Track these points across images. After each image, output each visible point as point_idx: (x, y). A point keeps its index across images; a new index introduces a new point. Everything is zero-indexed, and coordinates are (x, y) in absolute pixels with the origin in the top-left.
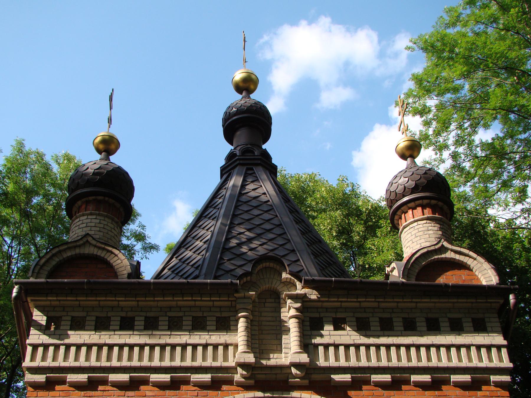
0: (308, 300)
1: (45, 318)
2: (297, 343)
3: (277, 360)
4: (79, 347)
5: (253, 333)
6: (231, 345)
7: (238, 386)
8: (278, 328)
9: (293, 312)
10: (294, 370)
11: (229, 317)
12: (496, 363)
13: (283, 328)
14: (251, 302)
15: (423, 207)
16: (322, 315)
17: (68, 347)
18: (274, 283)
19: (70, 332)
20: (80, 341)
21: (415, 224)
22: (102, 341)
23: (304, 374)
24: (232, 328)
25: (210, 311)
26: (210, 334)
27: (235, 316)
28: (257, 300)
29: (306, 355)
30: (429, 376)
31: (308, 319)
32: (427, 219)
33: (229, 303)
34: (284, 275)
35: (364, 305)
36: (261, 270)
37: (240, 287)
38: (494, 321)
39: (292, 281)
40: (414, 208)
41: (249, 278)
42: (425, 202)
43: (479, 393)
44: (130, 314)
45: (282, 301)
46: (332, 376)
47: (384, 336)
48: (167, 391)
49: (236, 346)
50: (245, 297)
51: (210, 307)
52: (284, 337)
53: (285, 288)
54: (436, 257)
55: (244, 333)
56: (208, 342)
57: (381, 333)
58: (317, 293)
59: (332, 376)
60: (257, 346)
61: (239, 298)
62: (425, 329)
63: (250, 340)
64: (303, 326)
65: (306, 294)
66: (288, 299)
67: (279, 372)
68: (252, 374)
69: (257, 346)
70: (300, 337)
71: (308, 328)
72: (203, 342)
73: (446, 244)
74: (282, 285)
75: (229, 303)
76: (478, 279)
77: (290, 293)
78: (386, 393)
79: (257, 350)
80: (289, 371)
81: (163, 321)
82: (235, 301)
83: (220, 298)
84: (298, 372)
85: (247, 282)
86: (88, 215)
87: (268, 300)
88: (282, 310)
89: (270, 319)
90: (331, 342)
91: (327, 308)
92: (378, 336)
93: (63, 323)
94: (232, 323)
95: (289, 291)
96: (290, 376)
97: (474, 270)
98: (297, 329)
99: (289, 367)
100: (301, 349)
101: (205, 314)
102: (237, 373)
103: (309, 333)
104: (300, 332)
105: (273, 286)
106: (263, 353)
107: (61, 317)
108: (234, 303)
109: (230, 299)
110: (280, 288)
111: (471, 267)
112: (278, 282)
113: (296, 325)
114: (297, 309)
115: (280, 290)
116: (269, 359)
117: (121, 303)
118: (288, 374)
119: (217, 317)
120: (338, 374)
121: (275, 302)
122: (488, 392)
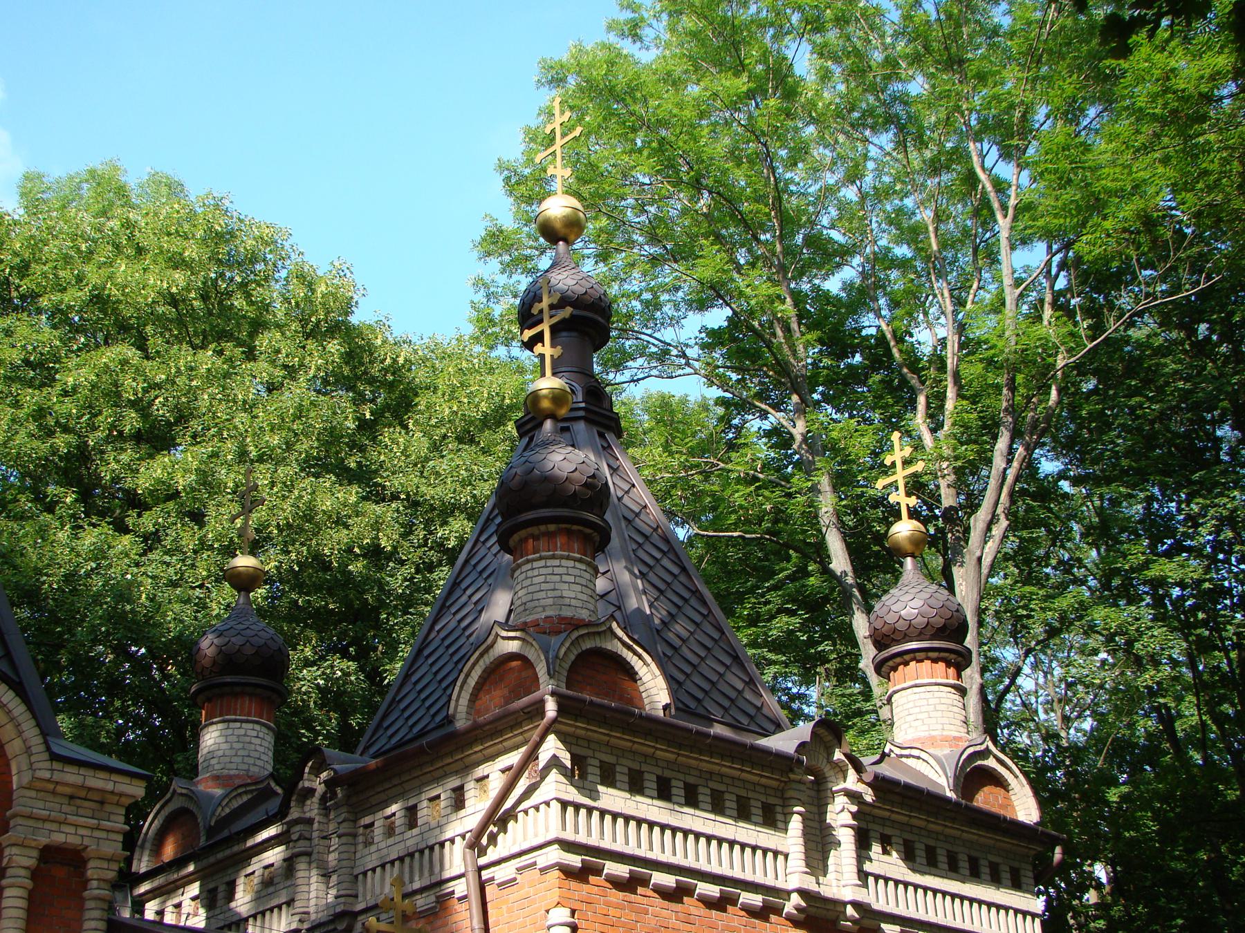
1: (568, 756)
4: (615, 816)
6: (781, 853)
9: (847, 818)
10: (850, 911)
17: (603, 813)
19: (601, 788)
24: (780, 825)
33: (774, 784)
44: (667, 774)
47: (930, 874)
48: (714, 912)
49: (786, 856)
50: (800, 782)
54: (979, 762)
57: (927, 869)
59: (883, 926)
61: (794, 781)
62: (967, 872)
81: (704, 796)
92: (923, 873)
93: (590, 769)
96: (842, 917)
99: (845, 904)
107: (585, 758)
110: (829, 772)
113: (852, 839)
117: (658, 752)
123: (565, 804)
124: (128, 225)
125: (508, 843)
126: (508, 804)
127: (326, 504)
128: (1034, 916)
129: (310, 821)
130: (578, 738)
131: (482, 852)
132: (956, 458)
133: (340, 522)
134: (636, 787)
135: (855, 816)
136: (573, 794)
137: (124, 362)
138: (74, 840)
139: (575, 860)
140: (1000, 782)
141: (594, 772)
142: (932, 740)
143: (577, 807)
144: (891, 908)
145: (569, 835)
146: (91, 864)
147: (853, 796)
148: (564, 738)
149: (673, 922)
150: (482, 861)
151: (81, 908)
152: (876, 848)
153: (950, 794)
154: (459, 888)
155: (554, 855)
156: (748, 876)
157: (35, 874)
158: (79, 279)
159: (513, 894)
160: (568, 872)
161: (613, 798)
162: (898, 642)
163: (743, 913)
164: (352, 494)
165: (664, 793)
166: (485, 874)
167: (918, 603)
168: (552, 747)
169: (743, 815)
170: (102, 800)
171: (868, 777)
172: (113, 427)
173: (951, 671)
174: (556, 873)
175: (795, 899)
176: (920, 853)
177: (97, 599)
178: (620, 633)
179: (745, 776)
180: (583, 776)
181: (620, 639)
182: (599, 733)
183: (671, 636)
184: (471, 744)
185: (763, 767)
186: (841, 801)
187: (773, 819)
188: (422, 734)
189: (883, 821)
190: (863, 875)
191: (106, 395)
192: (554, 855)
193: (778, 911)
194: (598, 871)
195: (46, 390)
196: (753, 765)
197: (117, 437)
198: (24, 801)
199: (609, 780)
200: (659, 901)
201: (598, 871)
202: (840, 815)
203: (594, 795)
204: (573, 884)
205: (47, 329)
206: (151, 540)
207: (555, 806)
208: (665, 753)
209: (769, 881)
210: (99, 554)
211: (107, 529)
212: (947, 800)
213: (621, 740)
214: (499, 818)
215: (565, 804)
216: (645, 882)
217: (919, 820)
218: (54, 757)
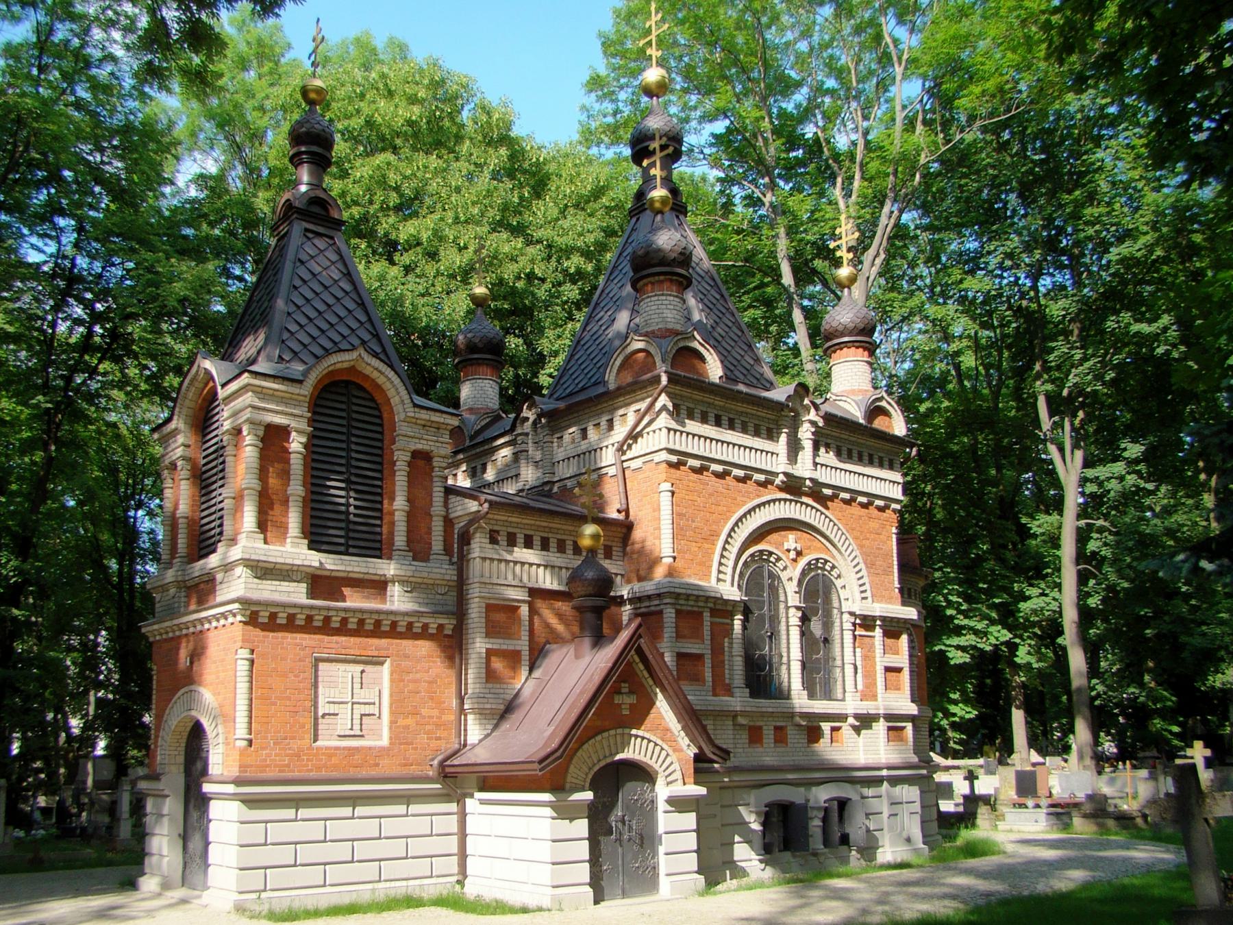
4: (694, 435)
10: (808, 483)
17: (688, 434)
44: (720, 413)
81: (738, 425)
110: (801, 411)
123: (669, 430)
124: (383, 76)
125: (638, 449)
126: (638, 429)
127: (506, 249)
129: (527, 434)
131: (624, 453)
132: (859, 218)
133: (514, 259)
134: (704, 420)
135: (813, 433)
136: (673, 425)
137: (389, 164)
138: (426, 448)
139: (674, 459)
141: (684, 412)
142: (853, 392)
143: (675, 431)
144: (828, 481)
145: (671, 446)
146: (436, 459)
147: (813, 423)
148: (670, 395)
149: (721, 489)
150: (624, 458)
151: (432, 481)
152: (822, 450)
153: (862, 421)
154: (612, 471)
155: (664, 456)
156: (759, 466)
157: (410, 464)
158: (358, 111)
159: (641, 476)
160: (671, 465)
161: (693, 426)
162: (838, 337)
164: (519, 243)
165: (718, 423)
166: (625, 464)
167: (851, 315)
168: (663, 400)
169: (757, 434)
170: (438, 427)
171: (822, 413)
172: (383, 202)
173: (866, 353)
174: (664, 465)
175: (781, 477)
176: (845, 453)
177: (383, 304)
180: (678, 415)
182: (686, 392)
183: (716, 335)
184: (618, 397)
185: (768, 409)
186: (806, 426)
187: (772, 436)
188: (583, 389)
189: (827, 436)
190: (815, 464)
191: (378, 183)
192: (664, 456)
193: (772, 483)
194: (685, 464)
195: (346, 181)
196: (764, 407)
197: (385, 209)
198: (402, 428)
199: (691, 417)
200: (714, 478)
201: (685, 464)
202: (806, 433)
203: (683, 425)
204: (673, 471)
205: (342, 143)
206: (408, 269)
207: (665, 431)
208: (719, 402)
209: (769, 468)
210: (382, 278)
211: (386, 263)
212: (861, 425)
213: (698, 395)
214: (634, 436)
215: (669, 430)
216: (707, 469)
217: (845, 435)
218: (415, 405)
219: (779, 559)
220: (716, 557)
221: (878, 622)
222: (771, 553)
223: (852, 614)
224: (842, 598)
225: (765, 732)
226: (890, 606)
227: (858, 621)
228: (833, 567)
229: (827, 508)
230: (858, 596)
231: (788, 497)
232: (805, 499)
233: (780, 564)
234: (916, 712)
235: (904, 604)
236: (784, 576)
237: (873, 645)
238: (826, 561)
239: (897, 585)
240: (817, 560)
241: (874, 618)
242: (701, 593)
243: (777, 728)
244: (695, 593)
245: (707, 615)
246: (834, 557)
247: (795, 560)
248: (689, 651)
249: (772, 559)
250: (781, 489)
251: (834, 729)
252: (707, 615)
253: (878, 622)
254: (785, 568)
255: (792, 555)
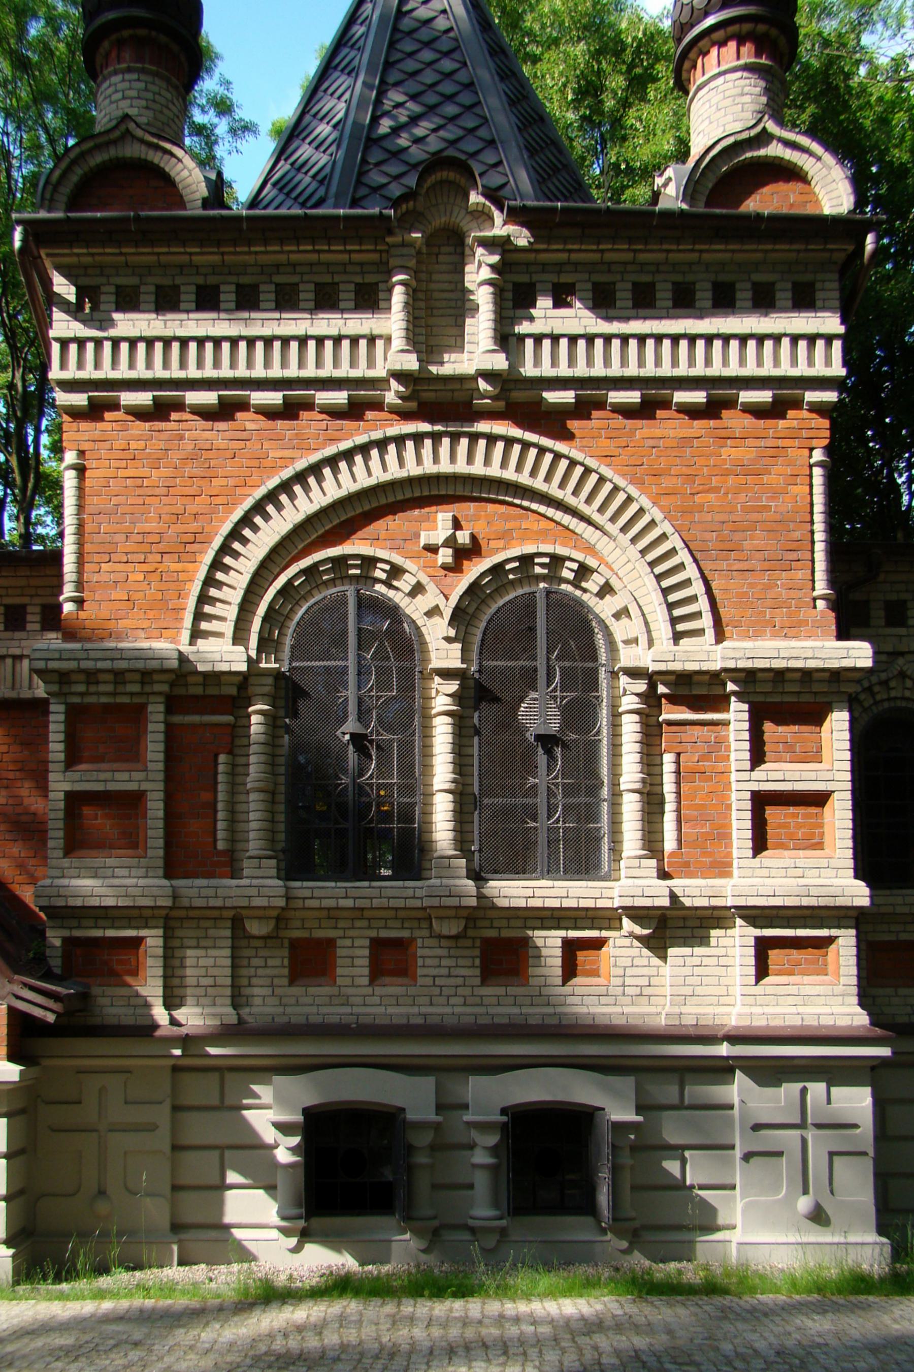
0: (512, 247)
2: (490, 333)
3: (455, 365)
4: (133, 342)
5: (418, 313)
6: (380, 337)
7: (391, 412)
8: (459, 303)
10: (483, 385)
11: (377, 284)
12: (820, 370)
13: (468, 305)
14: (413, 252)
15: (741, 41)
16: (535, 278)
17: (116, 342)
18: (455, 214)
19: (116, 316)
20: (134, 333)
21: (721, 80)
22: (169, 333)
23: (497, 391)
24: (382, 304)
25: (345, 272)
26: (345, 316)
27: (387, 282)
28: (424, 250)
29: (503, 356)
30: (704, 394)
31: (510, 287)
32: (747, 68)
33: (375, 257)
34: (475, 198)
35: (608, 257)
36: (433, 186)
37: (396, 224)
38: (830, 289)
39: (486, 210)
40: (722, 44)
41: (411, 204)
42: (747, 27)
43: (781, 423)
44: (212, 280)
45: (467, 251)
46: (546, 395)
47: (637, 318)
48: (279, 422)
49: (388, 339)
51: (345, 264)
52: (468, 321)
53: (474, 224)
55: (401, 315)
56: (342, 333)
57: (633, 312)
58: (529, 235)
59: (546, 395)
60: (422, 339)
63: (411, 328)
64: (502, 299)
65: (509, 236)
66: (479, 246)
67: (458, 386)
68: (414, 391)
69: (422, 339)
70: (495, 321)
71: (510, 304)
72: (334, 332)
73: (771, 127)
74: (468, 218)
75: (375, 257)
76: (817, 202)
77: (482, 234)
78: (629, 423)
79: (423, 348)
80: (474, 386)
81: (267, 294)
82: (388, 252)
83: (360, 244)
84: (489, 388)
85: (407, 212)
86: (123, 72)
87: (445, 249)
88: (468, 268)
89: (445, 286)
90: (547, 330)
91: (544, 265)
92: (627, 319)
94: (382, 295)
95: (481, 231)
96: (475, 395)
97: (813, 183)
98: (490, 307)
99: (473, 378)
100: (495, 344)
101: (337, 279)
102: (390, 390)
103: (510, 313)
104: (495, 312)
105: (453, 219)
106: (432, 352)
108: (384, 255)
109: (379, 248)
110: (464, 223)
111: (809, 178)
112: (463, 212)
114: (492, 267)
115: (465, 229)
116: (442, 363)
117: (194, 258)
118: (473, 390)
119: (357, 284)
120: (554, 390)
121: (456, 253)
122: (795, 422)
128: (829, 339)
130: (86, 268)
140: (793, 174)
143: (81, 342)
149: (220, 443)
163: (324, 416)
178: (139, 133)
179: (324, 257)
181: (142, 141)
182: (109, 254)
189: (559, 267)
203: (105, 323)
219: (396, 571)
220: (195, 589)
221: (731, 687)
222: (369, 562)
223: (634, 673)
224: (619, 637)
225: (340, 952)
226: (794, 643)
227: (662, 689)
228: (584, 571)
229: (567, 436)
230: (662, 629)
231: (425, 427)
232: (483, 427)
233: (405, 583)
234: (865, 902)
235: (843, 634)
236: (414, 609)
237: (721, 743)
238: (557, 561)
239: (821, 587)
240: (526, 560)
241: (716, 677)
242: (123, 665)
243: (378, 946)
244: (140, 665)
245: (156, 712)
246: (590, 549)
247: (455, 568)
248: (112, 786)
249: (380, 574)
250: (405, 415)
251: (570, 948)
252: (156, 712)
253: (731, 687)
254: (418, 589)
255: (445, 556)
